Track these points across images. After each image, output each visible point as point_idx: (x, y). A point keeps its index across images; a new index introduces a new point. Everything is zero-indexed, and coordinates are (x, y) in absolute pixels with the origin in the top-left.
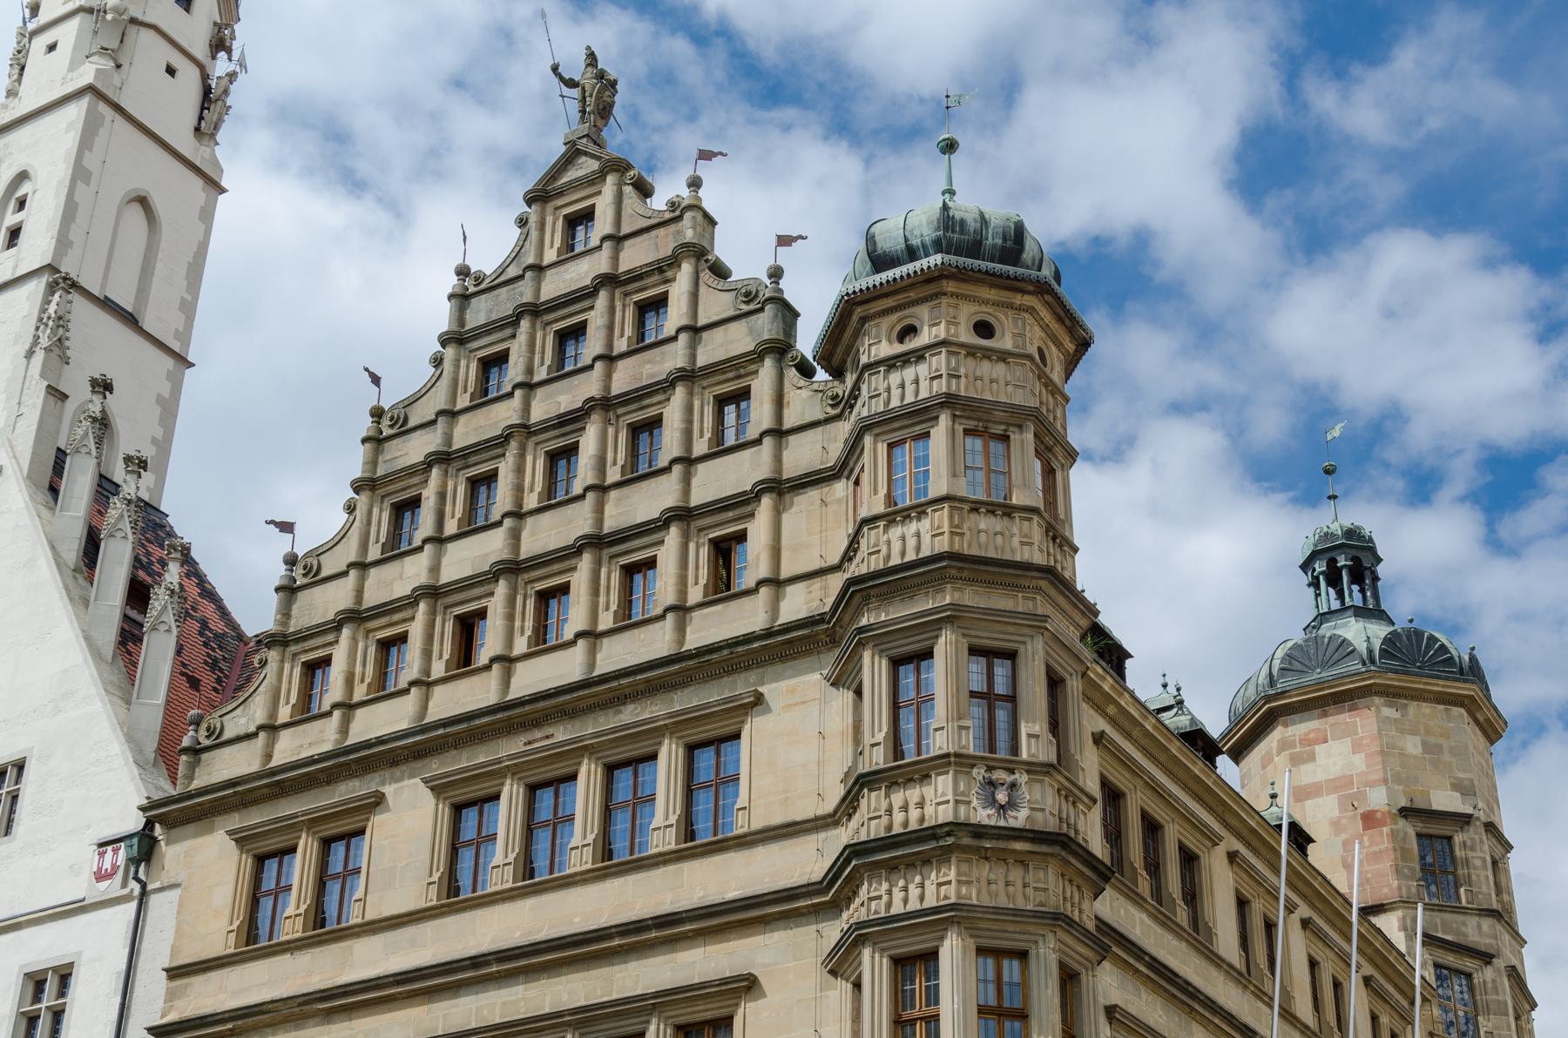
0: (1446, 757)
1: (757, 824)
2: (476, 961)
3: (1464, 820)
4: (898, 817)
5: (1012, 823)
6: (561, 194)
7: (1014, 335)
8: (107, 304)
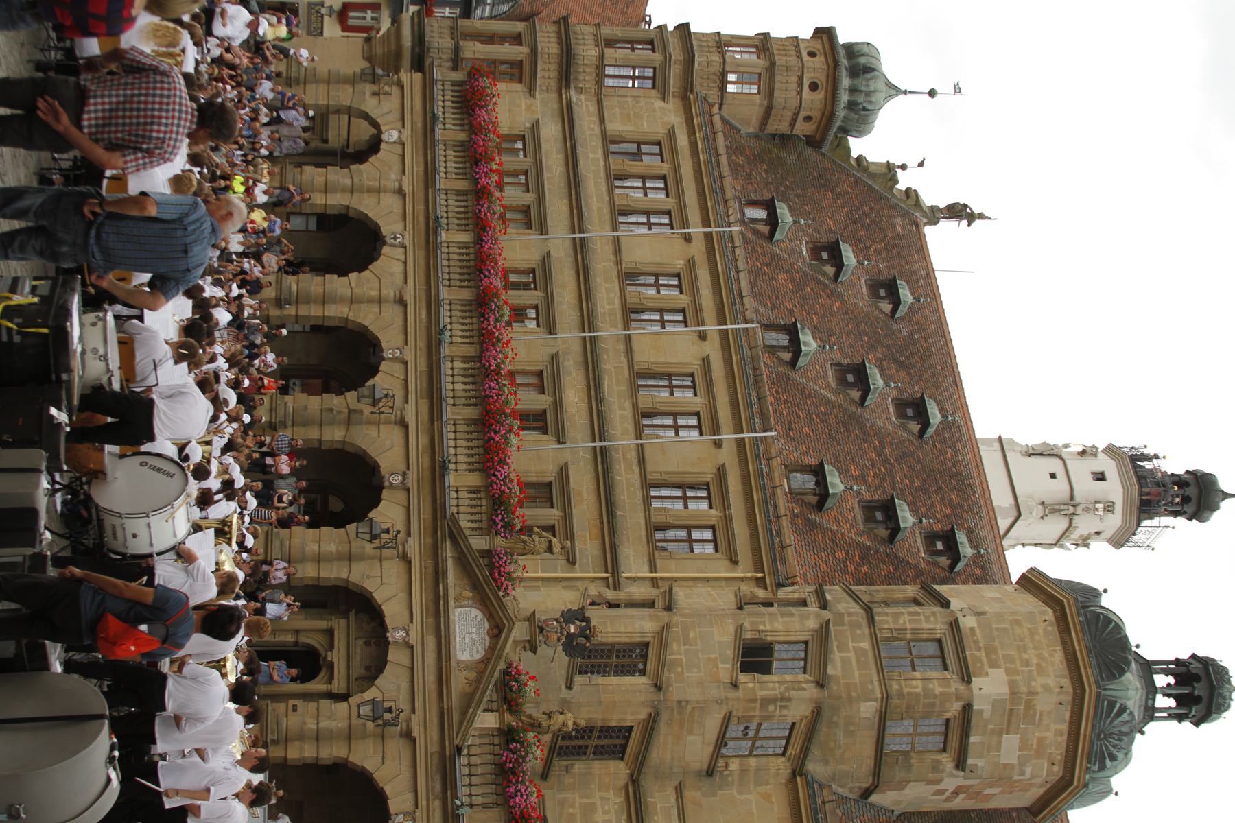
3: (945, 604)
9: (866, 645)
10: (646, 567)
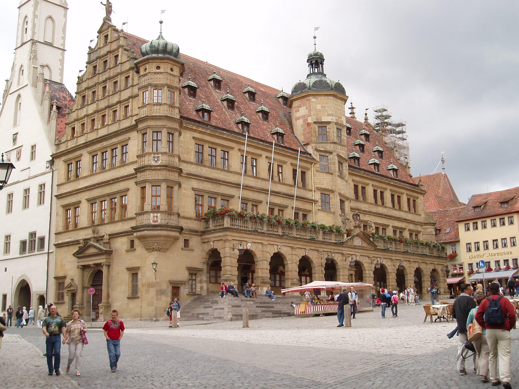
0: (326, 108)
1: (130, 161)
2: (94, 185)
3: (329, 123)
4: (142, 163)
5: (158, 164)
6: (103, 32)
7: (164, 68)
8: (46, 43)
9: (339, 147)
10: (311, 192)
